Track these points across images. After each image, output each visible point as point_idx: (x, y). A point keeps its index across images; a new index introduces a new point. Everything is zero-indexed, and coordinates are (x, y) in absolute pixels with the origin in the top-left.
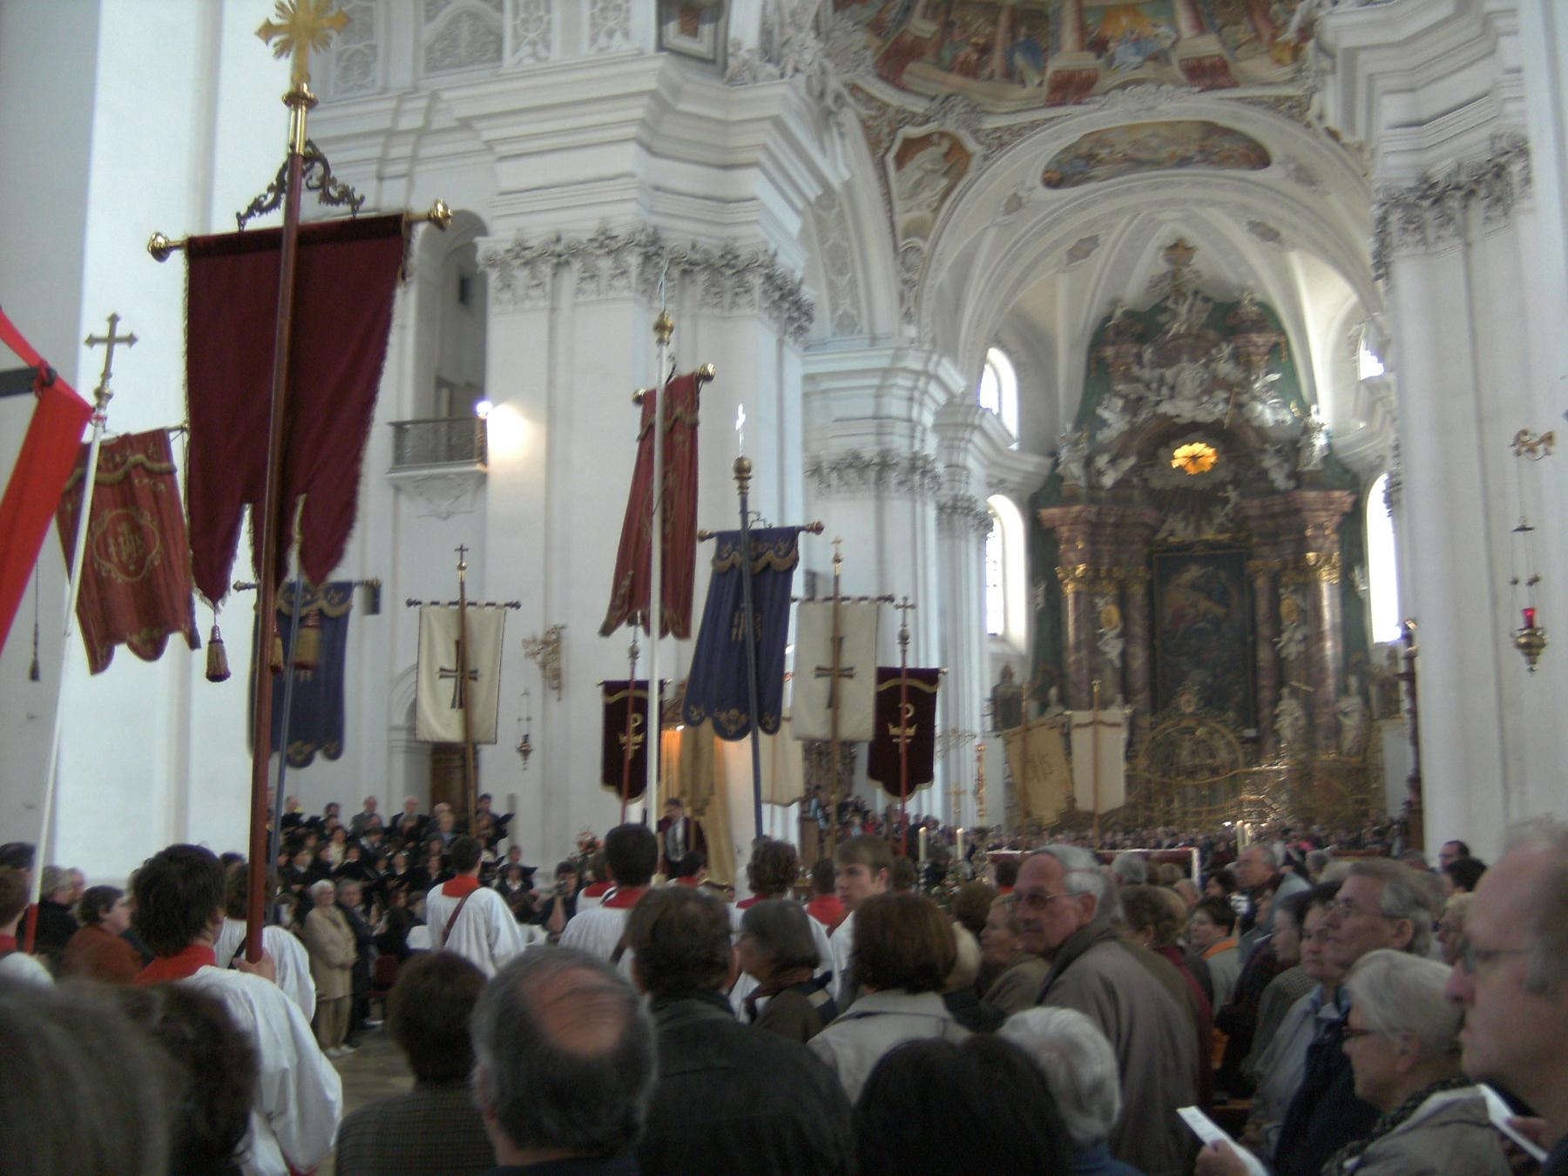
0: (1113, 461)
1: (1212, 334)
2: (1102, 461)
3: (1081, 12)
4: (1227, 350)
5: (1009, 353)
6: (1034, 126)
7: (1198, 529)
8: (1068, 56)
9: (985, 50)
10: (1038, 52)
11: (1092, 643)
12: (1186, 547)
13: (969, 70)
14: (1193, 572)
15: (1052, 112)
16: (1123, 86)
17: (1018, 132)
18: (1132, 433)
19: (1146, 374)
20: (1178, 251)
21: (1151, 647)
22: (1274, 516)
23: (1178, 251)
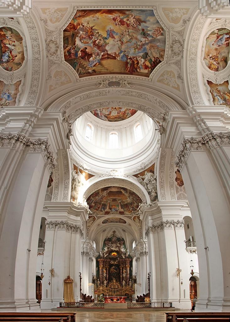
0: (106, 254)
1: (117, 241)
2: (105, 254)
3: (109, 205)
4: (118, 243)
5: (95, 242)
6: (103, 216)
7: (114, 262)
8: (107, 209)
9: (99, 208)
10: (104, 209)
11: (103, 274)
12: (112, 264)
13: (97, 210)
14: (114, 267)
15: (105, 215)
16: (112, 213)
17: (101, 217)
18: (108, 251)
19: (110, 245)
20: (114, 232)
21: (109, 275)
22: (123, 261)
23: (114, 232)
